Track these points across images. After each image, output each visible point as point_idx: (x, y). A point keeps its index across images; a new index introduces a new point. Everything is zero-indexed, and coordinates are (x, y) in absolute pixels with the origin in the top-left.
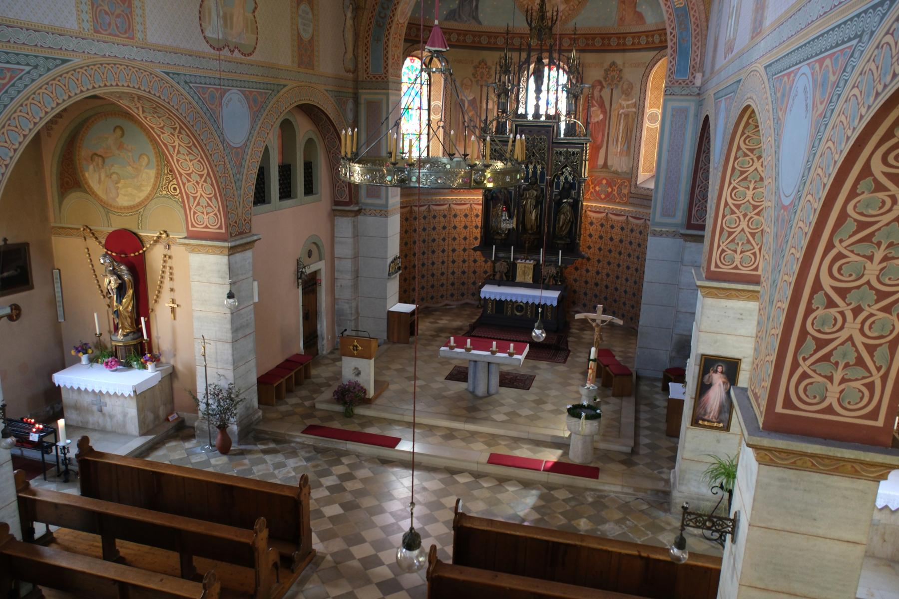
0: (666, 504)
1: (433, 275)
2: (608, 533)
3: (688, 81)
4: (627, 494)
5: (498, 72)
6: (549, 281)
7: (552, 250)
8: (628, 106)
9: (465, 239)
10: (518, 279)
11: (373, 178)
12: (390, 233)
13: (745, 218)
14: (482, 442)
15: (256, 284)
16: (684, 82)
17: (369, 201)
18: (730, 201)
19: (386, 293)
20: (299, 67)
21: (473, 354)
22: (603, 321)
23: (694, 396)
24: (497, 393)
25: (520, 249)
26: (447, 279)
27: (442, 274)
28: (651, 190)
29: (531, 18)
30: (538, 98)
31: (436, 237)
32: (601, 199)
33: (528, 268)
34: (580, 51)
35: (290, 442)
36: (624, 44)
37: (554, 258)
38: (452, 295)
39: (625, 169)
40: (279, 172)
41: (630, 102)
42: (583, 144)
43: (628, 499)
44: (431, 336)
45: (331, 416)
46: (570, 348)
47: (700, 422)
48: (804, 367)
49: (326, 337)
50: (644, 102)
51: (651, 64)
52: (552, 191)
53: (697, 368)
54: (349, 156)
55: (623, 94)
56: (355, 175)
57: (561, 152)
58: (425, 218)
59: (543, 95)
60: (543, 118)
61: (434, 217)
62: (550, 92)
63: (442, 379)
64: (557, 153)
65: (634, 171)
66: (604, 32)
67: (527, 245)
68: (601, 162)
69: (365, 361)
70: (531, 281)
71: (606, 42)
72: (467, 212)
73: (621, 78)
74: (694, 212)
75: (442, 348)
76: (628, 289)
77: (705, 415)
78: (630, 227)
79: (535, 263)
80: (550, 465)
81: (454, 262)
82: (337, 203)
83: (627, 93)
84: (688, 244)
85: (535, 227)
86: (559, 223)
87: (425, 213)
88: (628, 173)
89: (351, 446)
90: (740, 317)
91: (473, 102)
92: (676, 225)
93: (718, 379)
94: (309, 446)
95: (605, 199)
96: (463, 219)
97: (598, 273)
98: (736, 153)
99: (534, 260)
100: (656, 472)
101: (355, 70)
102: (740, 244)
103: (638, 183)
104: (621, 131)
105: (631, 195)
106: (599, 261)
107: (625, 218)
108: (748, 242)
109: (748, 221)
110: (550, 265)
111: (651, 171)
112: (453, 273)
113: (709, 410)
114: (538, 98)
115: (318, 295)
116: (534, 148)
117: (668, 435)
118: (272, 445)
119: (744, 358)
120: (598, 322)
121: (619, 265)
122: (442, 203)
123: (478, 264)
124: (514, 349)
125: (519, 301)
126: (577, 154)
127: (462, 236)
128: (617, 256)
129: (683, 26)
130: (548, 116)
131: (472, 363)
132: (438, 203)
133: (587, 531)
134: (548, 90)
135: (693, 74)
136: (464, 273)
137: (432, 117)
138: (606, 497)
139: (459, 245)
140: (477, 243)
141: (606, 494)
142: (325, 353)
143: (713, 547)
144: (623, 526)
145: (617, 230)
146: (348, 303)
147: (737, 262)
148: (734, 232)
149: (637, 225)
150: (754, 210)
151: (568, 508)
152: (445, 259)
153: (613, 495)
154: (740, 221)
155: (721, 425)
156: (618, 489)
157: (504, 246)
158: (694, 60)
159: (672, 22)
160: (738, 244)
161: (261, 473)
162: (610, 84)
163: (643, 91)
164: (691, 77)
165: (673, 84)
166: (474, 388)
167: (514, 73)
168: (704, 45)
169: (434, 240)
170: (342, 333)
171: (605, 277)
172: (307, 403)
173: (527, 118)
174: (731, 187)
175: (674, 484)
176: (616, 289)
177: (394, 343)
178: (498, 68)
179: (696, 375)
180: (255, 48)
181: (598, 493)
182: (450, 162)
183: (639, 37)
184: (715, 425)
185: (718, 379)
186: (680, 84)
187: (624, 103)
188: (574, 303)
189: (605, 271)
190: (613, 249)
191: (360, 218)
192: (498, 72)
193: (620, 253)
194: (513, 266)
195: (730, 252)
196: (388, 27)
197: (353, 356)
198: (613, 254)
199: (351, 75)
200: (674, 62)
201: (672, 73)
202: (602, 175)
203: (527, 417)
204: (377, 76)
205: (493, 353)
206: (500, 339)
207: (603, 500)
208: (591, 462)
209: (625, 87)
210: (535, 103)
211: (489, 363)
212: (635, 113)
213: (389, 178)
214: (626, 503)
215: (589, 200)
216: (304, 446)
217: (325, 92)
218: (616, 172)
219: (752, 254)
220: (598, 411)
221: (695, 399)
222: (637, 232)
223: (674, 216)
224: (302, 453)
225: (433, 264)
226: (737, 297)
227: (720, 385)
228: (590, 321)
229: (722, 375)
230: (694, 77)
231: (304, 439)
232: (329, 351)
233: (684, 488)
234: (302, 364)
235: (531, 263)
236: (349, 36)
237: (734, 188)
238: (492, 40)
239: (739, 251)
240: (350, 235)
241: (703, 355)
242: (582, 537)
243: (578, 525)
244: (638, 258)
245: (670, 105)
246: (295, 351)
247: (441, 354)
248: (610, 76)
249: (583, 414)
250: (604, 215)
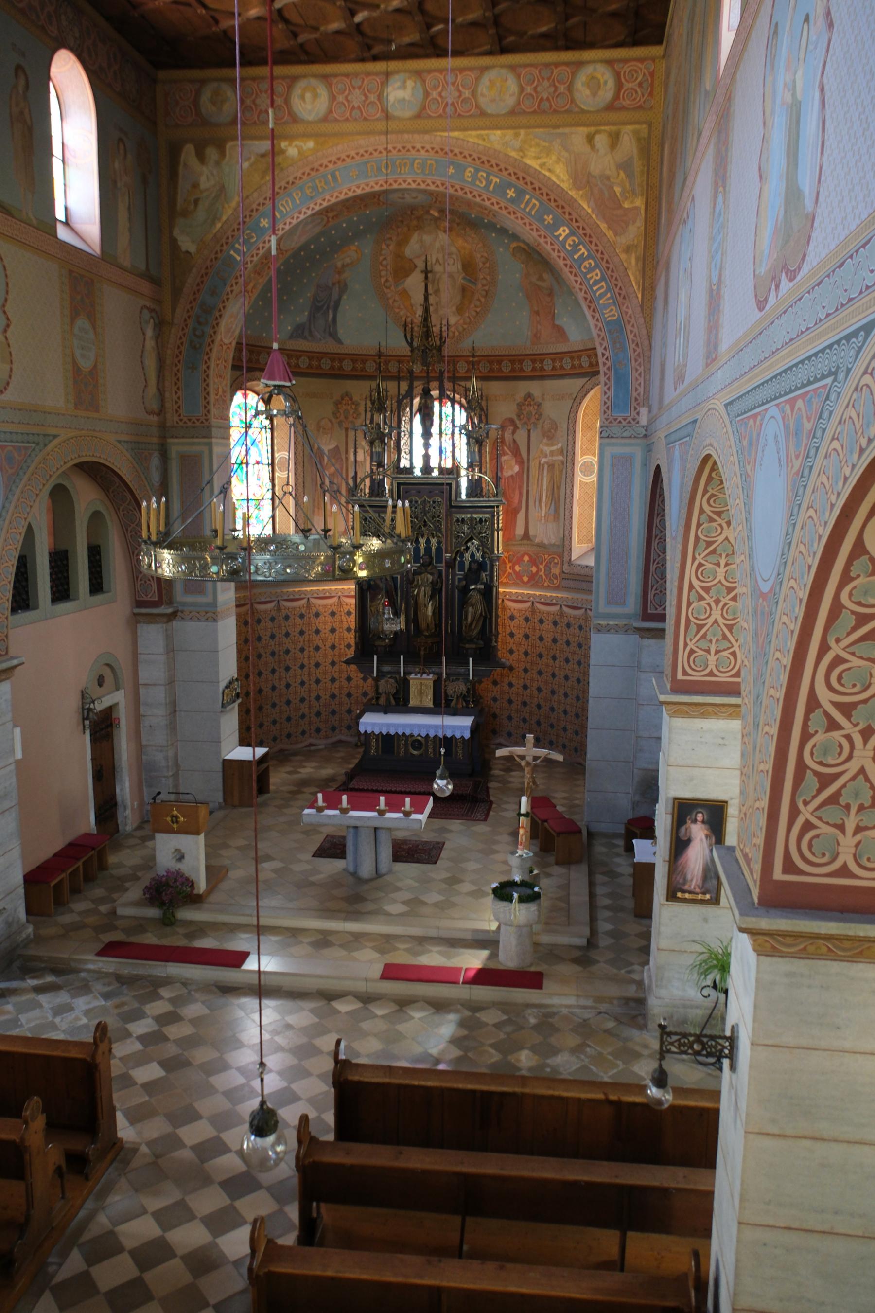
0: (640, 1018)
1: (288, 702)
2: (561, 1069)
3: (629, 419)
4: (585, 1007)
5: (369, 409)
6: (457, 703)
7: (458, 657)
8: (552, 453)
9: (333, 647)
10: (413, 702)
11: (191, 569)
12: (221, 646)
13: (717, 606)
14: (372, 948)
15: (17, 731)
16: (625, 420)
17: (190, 599)
18: (696, 583)
19: (219, 733)
20: (76, 408)
21: (351, 817)
22: (535, 758)
23: (667, 858)
24: (390, 872)
25: (413, 659)
26: (310, 708)
27: (303, 700)
28: (591, 568)
29: (412, 335)
30: (427, 446)
31: (291, 647)
32: (523, 582)
33: (426, 685)
34: (482, 378)
35: (78, 971)
36: (542, 369)
37: (462, 670)
38: (318, 730)
39: (553, 542)
40: (50, 562)
41: (554, 448)
42: (493, 507)
43: (587, 1014)
44: (290, 792)
45: (141, 925)
46: (492, 798)
47: (679, 895)
48: (806, 814)
49: (129, 803)
50: (574, 447)
51: (580, 395)
52: (454, 575)
53: (669, 817)
54: (154, 538)
55: (544, 436)
56: (164, 566)
57: (463, 519)
58: (272, 619)
59: (434, 441)
60: (436, 473)
61: (287, 618)
62: (444, 435)
63: (308, 856)
64: (458, 521)
65: (567, 542)
66: (514, 353)
67: (422, 653)
68: (520, 531)
69: (190, 838)
70: (429, 702)
71: (517, 366)
72: (335, 609)
73: (541, 415)
74: (650, 596)
75: (307, 811)
77: (684, 884)
79: (436, 677)
80: (472, 974)
81: (318, 681)
82: (139, 604)
83: (550, 435)
84: (647, 642)
85: (433, 626)
86: (466, 619)
87: (274, 613)
88: (558, 546)
89: (174, 969)
90: (721, 742)
91: (335, 452)
92: (627, 616)
93: (698, 832)
94: (108, 975)
95: (528, 582)
96: (329, 619)
97: (525, 687)
98: (699, 518)
99: (434, 673)
100: (623, 971)
101: (161, 411)
102: (714, 641)
104: (545, 487)
105: (564, 576)
106: (526, 670)
107: (558, 607)
108: (725, 637)
109: (722, 609)
110: (458, 679)
111: (590, 541)
112: (318, 698)
113: (689, 877)
114: (427, 446)
115: (115, 741)
116: (425, 515)
117: (636, 916)
118: (50, 979)
119: (731, 799)
120: (529, 759)
121: (554, 675)
122: (297, 597)
123: (353, 683)
124: (412, 805)
125: (415, 733)
126: (486, 521)
127: (329, 644)
128: (551, 662)
129: (618, 345)
130: (442, 470)
131: (351, 830)
132: (291, 597)
133: (530, 1069)
134: (441, 434)
135: (635, 409)
136: (333, 696)
137: (277, 474)
138: (555, 1014)
139: (325, 656)
140: (351, 653)
141: (555, 1010)
142: (129, 828)
143: (710, 1074)
144: (583, 1057)
145: (548, 625)
146: (161, 751)
147: (712, 666)
148: (705, 625)
149: (575, 617)
150: (728, 593)
151: (502, 1036)
152: (306, 679)
153: (565, 1011)
154: (711, 609)
155: (708, 896)
156: (572, 1001)
157: (389, 655)
158: (636, 390)
159: (603, 339)
160: (711, 641)
161: (32, 1024)
162: (525, 423)
163: (571, 432)
164: (634, 413)
165: (611, 422)
166: (356, 866)
167: (391, 411)
168: (648, 370)
169: (287, 652)
170: (154, 799)
171: (535, 692)
172: (103, 909)
173: (412, 473)
174: (696, 563)
175: (650, 987)
176: (552, 709)
177: (234, 807)
178: (369, 404)
179: (669, 827)
180: (8, 384)
181: (543, 1010)
182: (304, 540)
183: (561, 359)
184: (700, 897)
185: (698, 832)
186: (620, 422)
187: (547, 450)
188: (494, 732)
189: (535, 685)
190: (544, 652)
191: (175, 624)
192: (369, 409)
193: (554, 658)
194: (404, 685)
195: (701, 652)
196: (208, 349)
197: (171, 831)
198: (544, 660)
199: (154, 419)
200: (609, 394)
201: (608, 408)
202: (523, 549)
203: (436, 905)
204: (194, 419)
205: (381, 813)
206: (391, 792)
207: (550, 1020)
208: (531, 965)
209: (546, 427)
210: (424, 452)
211: (376, 829)
212: (562, 462)
213: (214, 569)
214: (585, 1021)
215: (506, 585)
216: (100, 975)
217: (118, 444)
218: (541, 545)
219: (730, 653)
220: (536, 889)
221: (670, 862)
222: (576, 626)
223: (624, 603)
224: (98, 987)
225: (288, 686)
226: (716, 715)
227: (701, 840)
228: (516, 758)
229: (703, 826)
230: (638, 414)
231: (100, 965)
232: (135, 826)
233: (663, 992)
234: (93, 849)
235: (429, 679)
236: (151, 363)
237: (700, 565)
238: (359, 365)
239: (713, 651)
240: (161, 650)
241: (675, 799)
242: (524, 1080)
243: (518, 1060)
244: (579, 663)
245: (608, 451)
246: (82, 830)
247: (305, 820)
248: (525, 413)
249: (516, 895)
250: (529, 604)
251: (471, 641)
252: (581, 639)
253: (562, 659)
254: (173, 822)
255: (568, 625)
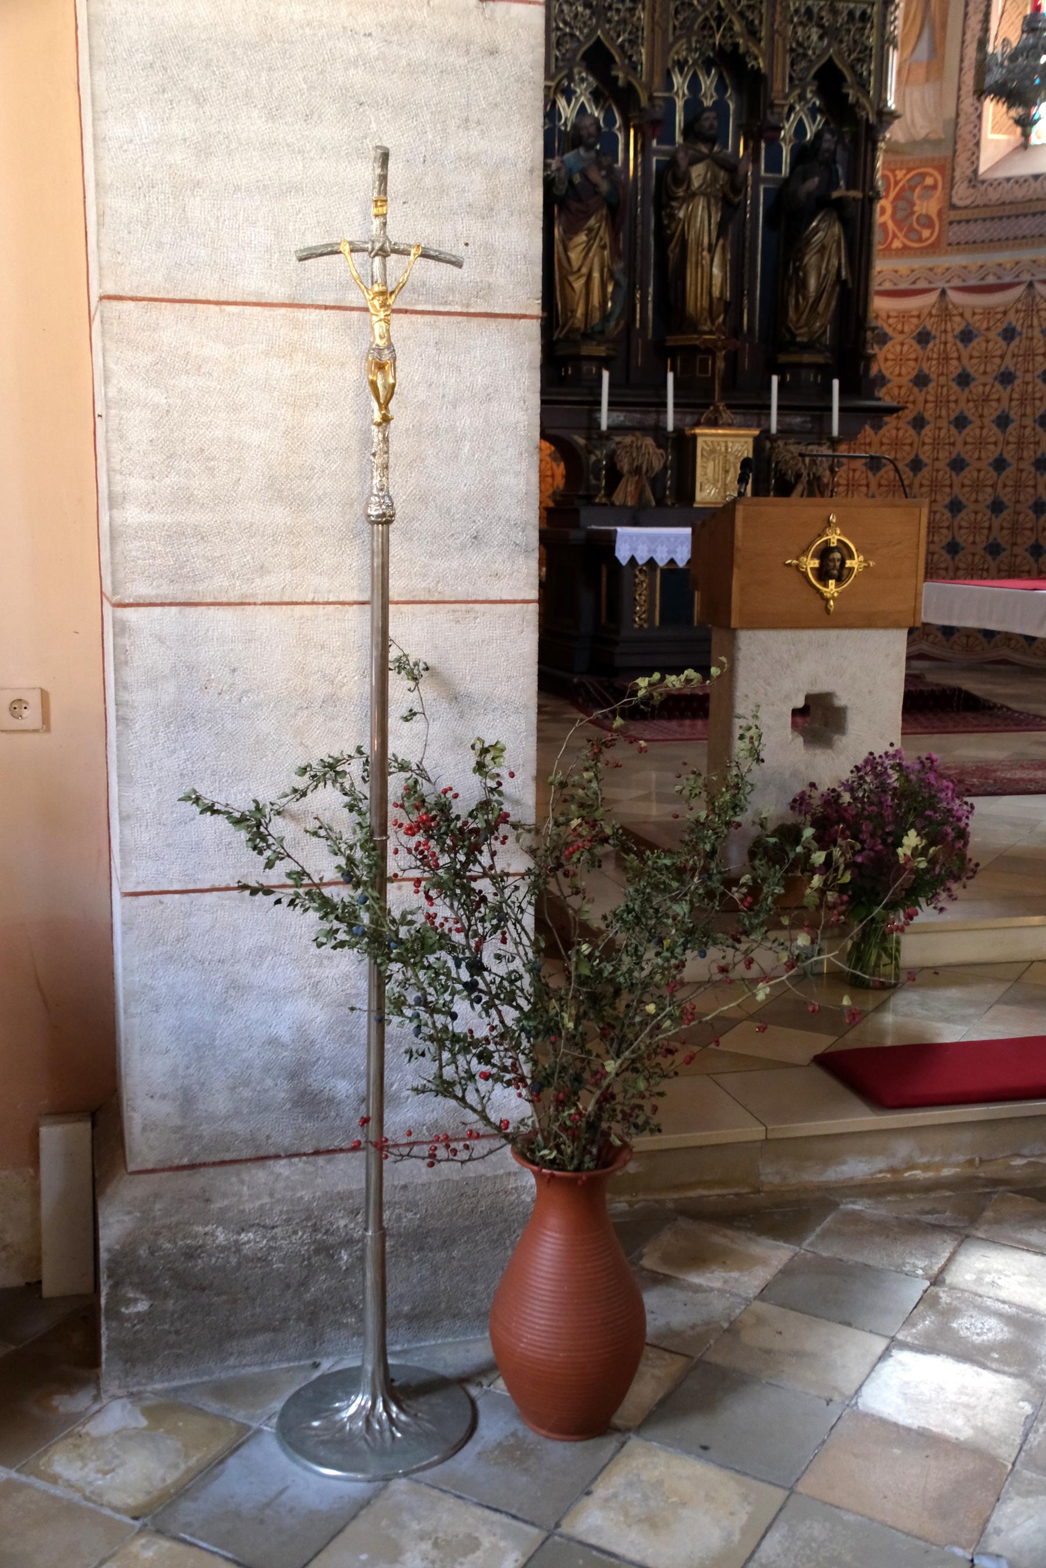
65: (965, 131)
76: (963, 538)
78: (957, 325)
86: (803, 284)
88: (937, 143)
103: (982, 168)
105: (953, 215)
107: (932, 298)
231: (903, 1149)
251: (805, 347)
252: (1009, 363)
253: (944, 423)
254: (823, 575)
255: (966, 336)
